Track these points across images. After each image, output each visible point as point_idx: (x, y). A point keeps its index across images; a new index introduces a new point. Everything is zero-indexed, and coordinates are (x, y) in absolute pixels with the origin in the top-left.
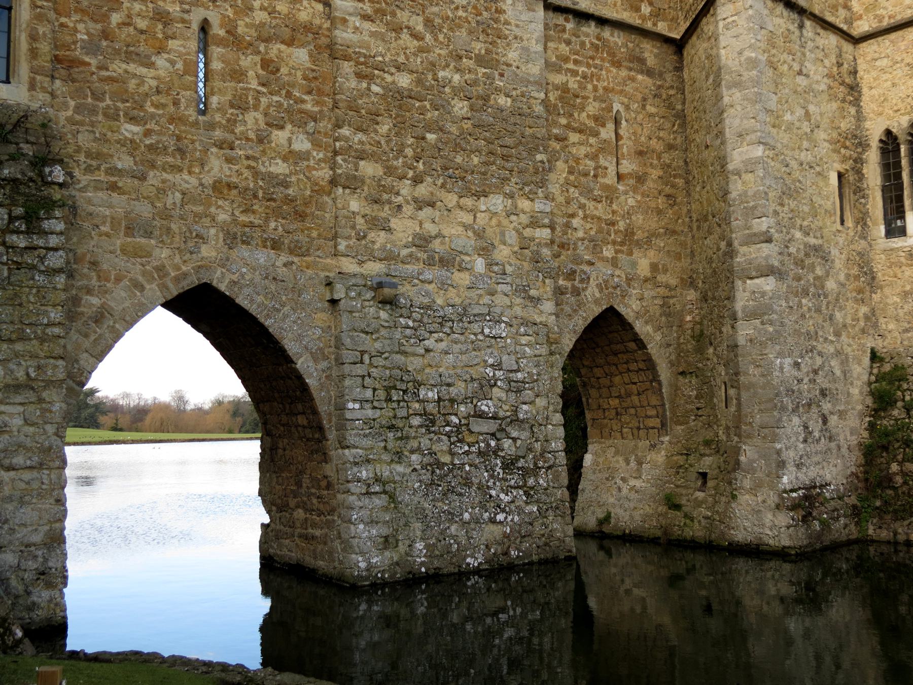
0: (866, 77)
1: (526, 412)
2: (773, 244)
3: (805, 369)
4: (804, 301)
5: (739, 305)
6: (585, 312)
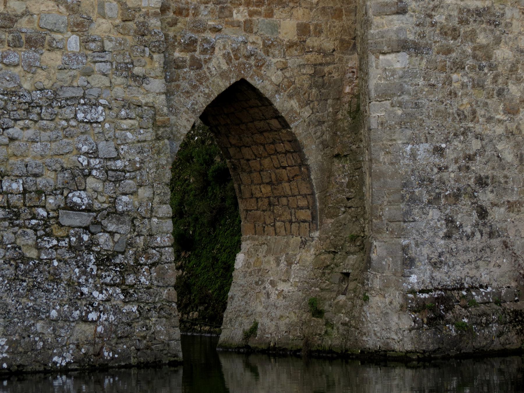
1: (127, 204)
2: (407, 16)
3: (451, 155)
4: (455, 76)
5: (373, 83)
6: (208, 87)
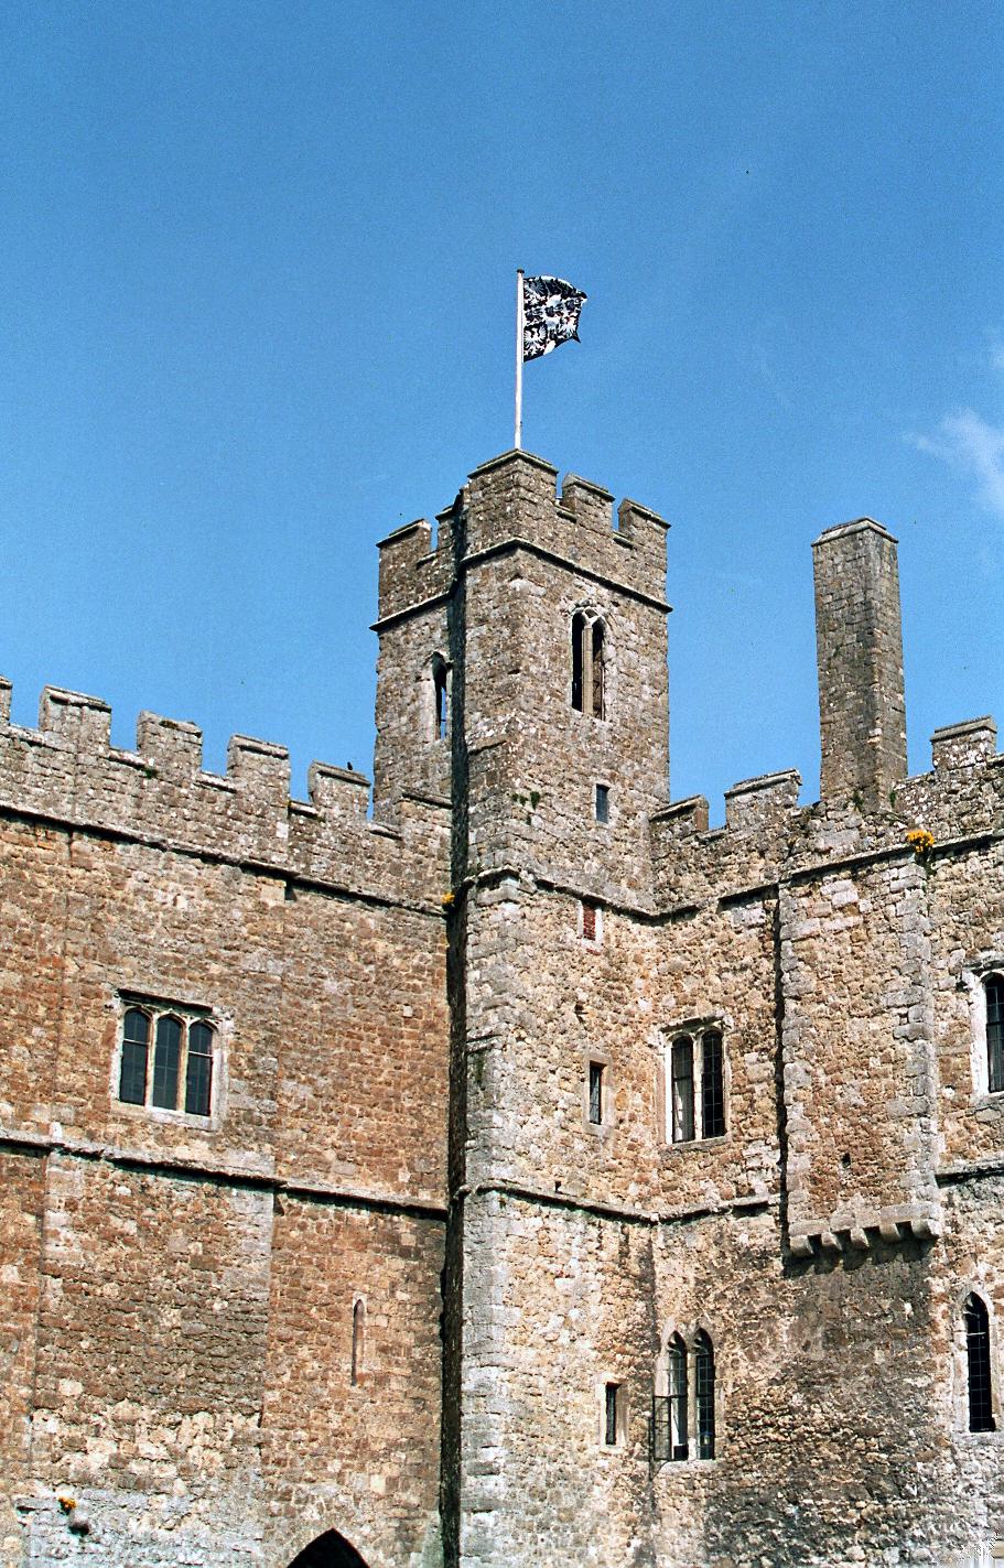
0: (660, 1268)
4: (540, 1536)
